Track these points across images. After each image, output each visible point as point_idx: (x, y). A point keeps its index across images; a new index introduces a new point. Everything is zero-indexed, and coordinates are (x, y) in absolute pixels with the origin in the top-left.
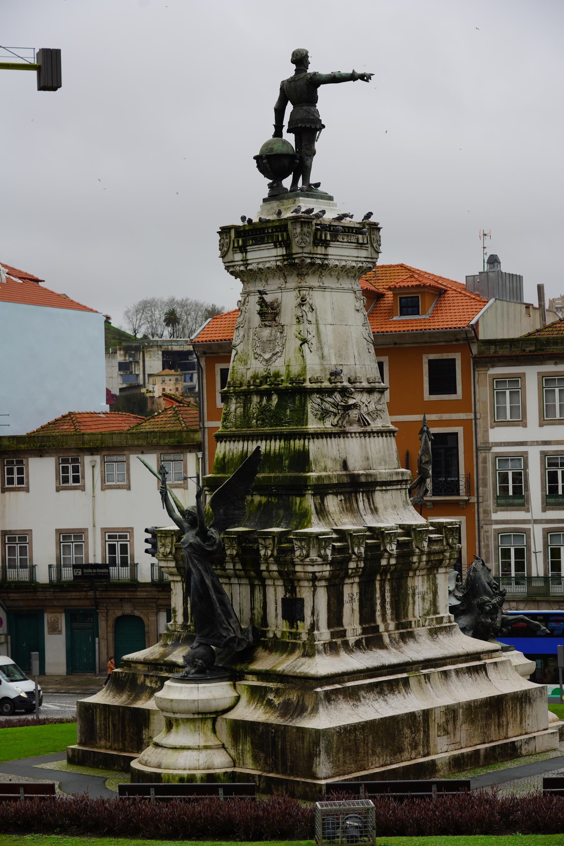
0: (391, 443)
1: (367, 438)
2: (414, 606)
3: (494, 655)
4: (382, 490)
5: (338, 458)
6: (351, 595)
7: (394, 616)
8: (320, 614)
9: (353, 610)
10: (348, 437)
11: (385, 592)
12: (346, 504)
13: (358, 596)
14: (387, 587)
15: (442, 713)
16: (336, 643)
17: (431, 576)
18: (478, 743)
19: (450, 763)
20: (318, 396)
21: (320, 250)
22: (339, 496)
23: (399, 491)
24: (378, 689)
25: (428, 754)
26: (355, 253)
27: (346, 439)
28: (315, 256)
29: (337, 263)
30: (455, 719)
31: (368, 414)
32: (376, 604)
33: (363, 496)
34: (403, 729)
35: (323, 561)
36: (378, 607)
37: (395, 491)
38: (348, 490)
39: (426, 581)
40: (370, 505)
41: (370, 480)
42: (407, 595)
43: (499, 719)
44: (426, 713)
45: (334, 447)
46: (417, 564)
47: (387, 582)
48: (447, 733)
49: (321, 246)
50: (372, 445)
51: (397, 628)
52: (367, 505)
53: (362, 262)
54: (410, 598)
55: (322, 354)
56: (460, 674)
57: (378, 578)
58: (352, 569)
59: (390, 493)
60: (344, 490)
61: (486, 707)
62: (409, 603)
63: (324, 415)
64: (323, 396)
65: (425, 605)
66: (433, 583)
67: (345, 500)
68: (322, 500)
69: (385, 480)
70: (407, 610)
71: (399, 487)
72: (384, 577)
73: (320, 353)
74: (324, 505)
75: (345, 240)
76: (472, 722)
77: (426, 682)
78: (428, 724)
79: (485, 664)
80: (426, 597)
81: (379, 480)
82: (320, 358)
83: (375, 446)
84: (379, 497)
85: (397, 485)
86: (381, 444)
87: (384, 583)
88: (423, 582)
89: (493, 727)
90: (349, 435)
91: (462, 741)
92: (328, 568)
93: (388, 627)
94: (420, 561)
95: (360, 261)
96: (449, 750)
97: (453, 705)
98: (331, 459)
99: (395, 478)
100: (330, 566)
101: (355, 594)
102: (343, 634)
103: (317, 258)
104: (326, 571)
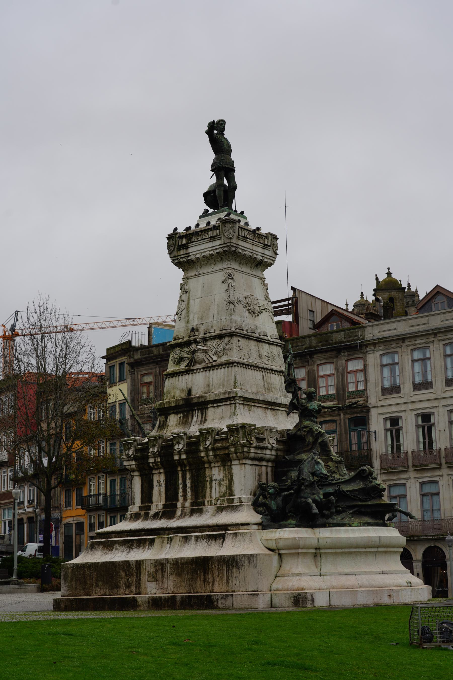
0: (232, 371)
1: (211, 372)
2: (211, 490)
3: (241, 527)
4: (214, 407)
5: (185, 389)
6: (159, 482)
7: (193, 497)
8: (136, 494)
9: (160, 492)
10: (195, 373)
11: (186, 479)
12: (183, 419)
13: (164, 482)
14: (188, 476)
15: (152, 565)
16: (140, 514)
17: (227, 467)
18: (184, 592)
19: (149, 602)
20: (178, 349)
22: (178, 414)
23: (229, 406)
24: (129, 545)
25: (140, 593)
26: (210, 244)
27: (194, 375)
28: (179, 257)
29: (198, 256)
30: (163, 570)
31: (216, 354)
32: (179, 488)
33: (198, 412)
34: (119, 572)
35: (128, 458)
36: (181, 490)
37: (226, 406)
38: (185, 409)
39: (222, 471)
40: (202, 418)
41: (200, 400)
42: (205, 481)
43: (204, 576)
44: (139, 563)
45: (183, 382)
46: (206, 458)
47: (188, 472)
48: (156, 580)
49: (183, 249)
50: (215, 375)
51: (192, 504)
52: (200, 418)
53: (219, 248)
54: (208, 484)
55: (188, 320)
56: (199, 540)
57: (179, 469)
58: (152, 463)
59: (221, 408)
60: (182, 410)
61: (192, 565)
62: (207, 487)
63: (180, 360)
64: (182, 348)
65: (222, 489)
66: (228, 473)
67: (183, 417)
68: (166, 418)
69: (213, 399)
70: (205, 493)
71: (228, 403)
72: (183, 469)
73: (186, 320)
74: (166, 421)
75: (199, 239)
76: (179, 575)
77: (168, 543)
78: (140, 571)
79: (224, 534)
80: (222, 483)
81: (208, 400)
82: (185, 323)
83: (217, 375)
84: (211, 412)
85: (227, 401)
86: (222, 373)
87: (186, 473)
88: (219, 471)
89: (198, 582)
90: (195, 371)
91: (169, 588)
92: (134, 463)
93: (184, 504)
94: (208, 456)
95: (217, 249)
96: (157, 593)
97: (162, 560)
98: (180, 390)
99: (222, 397)
100: (135, 461)
101: (162, 481)
102: (149, 508)
103: (182, 258)
104: (133, 465)
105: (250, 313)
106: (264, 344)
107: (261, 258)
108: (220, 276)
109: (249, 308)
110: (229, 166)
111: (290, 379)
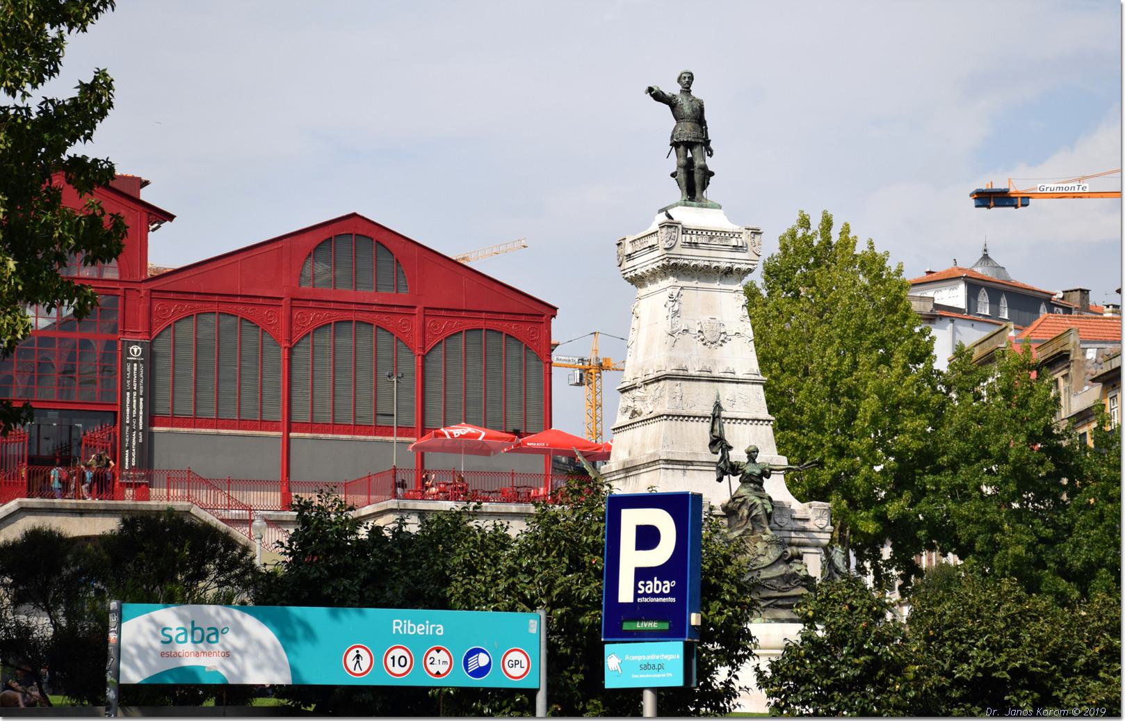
21: (631, 263)
71: (654, 468)
105: (705, 344)
106: (726, 384)
107: (729, 265)
108: (664, 297)
109: (702, 337)
110: (689, 139)
111: (714, 436)
